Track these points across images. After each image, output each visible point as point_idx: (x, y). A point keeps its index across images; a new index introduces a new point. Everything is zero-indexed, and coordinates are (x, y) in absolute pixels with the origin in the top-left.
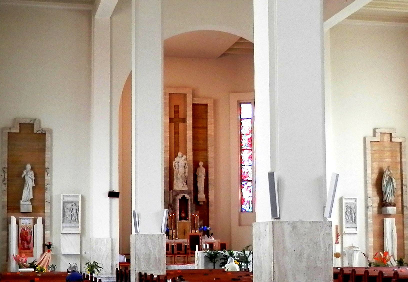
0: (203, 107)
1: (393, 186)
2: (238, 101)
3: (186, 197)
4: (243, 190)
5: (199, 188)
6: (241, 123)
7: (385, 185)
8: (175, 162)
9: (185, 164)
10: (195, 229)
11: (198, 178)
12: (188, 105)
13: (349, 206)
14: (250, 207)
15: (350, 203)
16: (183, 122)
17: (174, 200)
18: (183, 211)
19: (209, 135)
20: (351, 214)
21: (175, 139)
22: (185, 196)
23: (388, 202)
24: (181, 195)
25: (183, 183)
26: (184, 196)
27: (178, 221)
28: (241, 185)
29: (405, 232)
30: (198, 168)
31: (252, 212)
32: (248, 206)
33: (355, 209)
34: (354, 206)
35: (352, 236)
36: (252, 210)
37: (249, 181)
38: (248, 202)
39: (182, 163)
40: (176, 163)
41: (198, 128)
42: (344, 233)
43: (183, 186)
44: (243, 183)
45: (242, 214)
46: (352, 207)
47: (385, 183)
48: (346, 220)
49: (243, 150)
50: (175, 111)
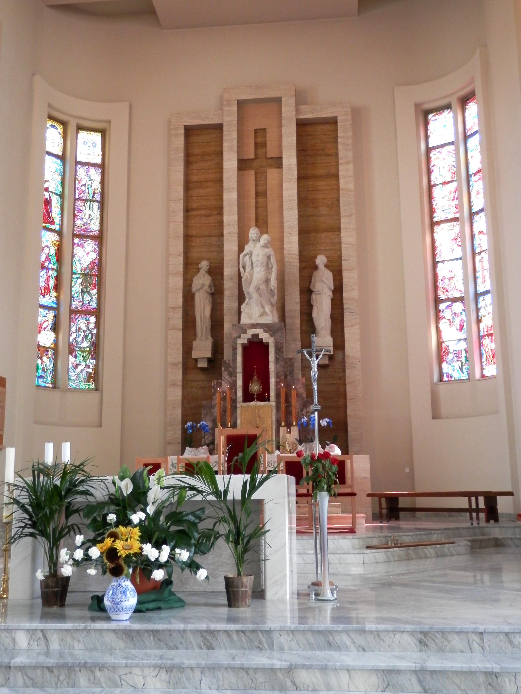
0: (329, 127)
2: (417, 106)
3: (262, 339)
4: (443, 325)
5: (316, 323)
6: (428, 160)
8: (245, 256)
9: (269, 257)
10: (289, 425)
11: (314, 296)
12: (284, 122)
14: (464, 367)
16: (278, 168)
17: (235, 349)
18: (255, 377)
19: (342, 190)
21: (257, 208)
22: (258, 335)
24: (251, 332)
25: (263, 307)
26: (256, 336)
27: (240, 404)
28: (437, 311)
30: (315, 273)
31: (469, 379)
32: (458, 364)
36: (469, 374)
37: (454, 300)
38: (457, 355)
39: (258, 255)
40: (247, 258)
41: (316, 177)
43: (263, 314)
44: (442, 306)
45: (442, 387)
49: (438, 223)
50: (256, 144)
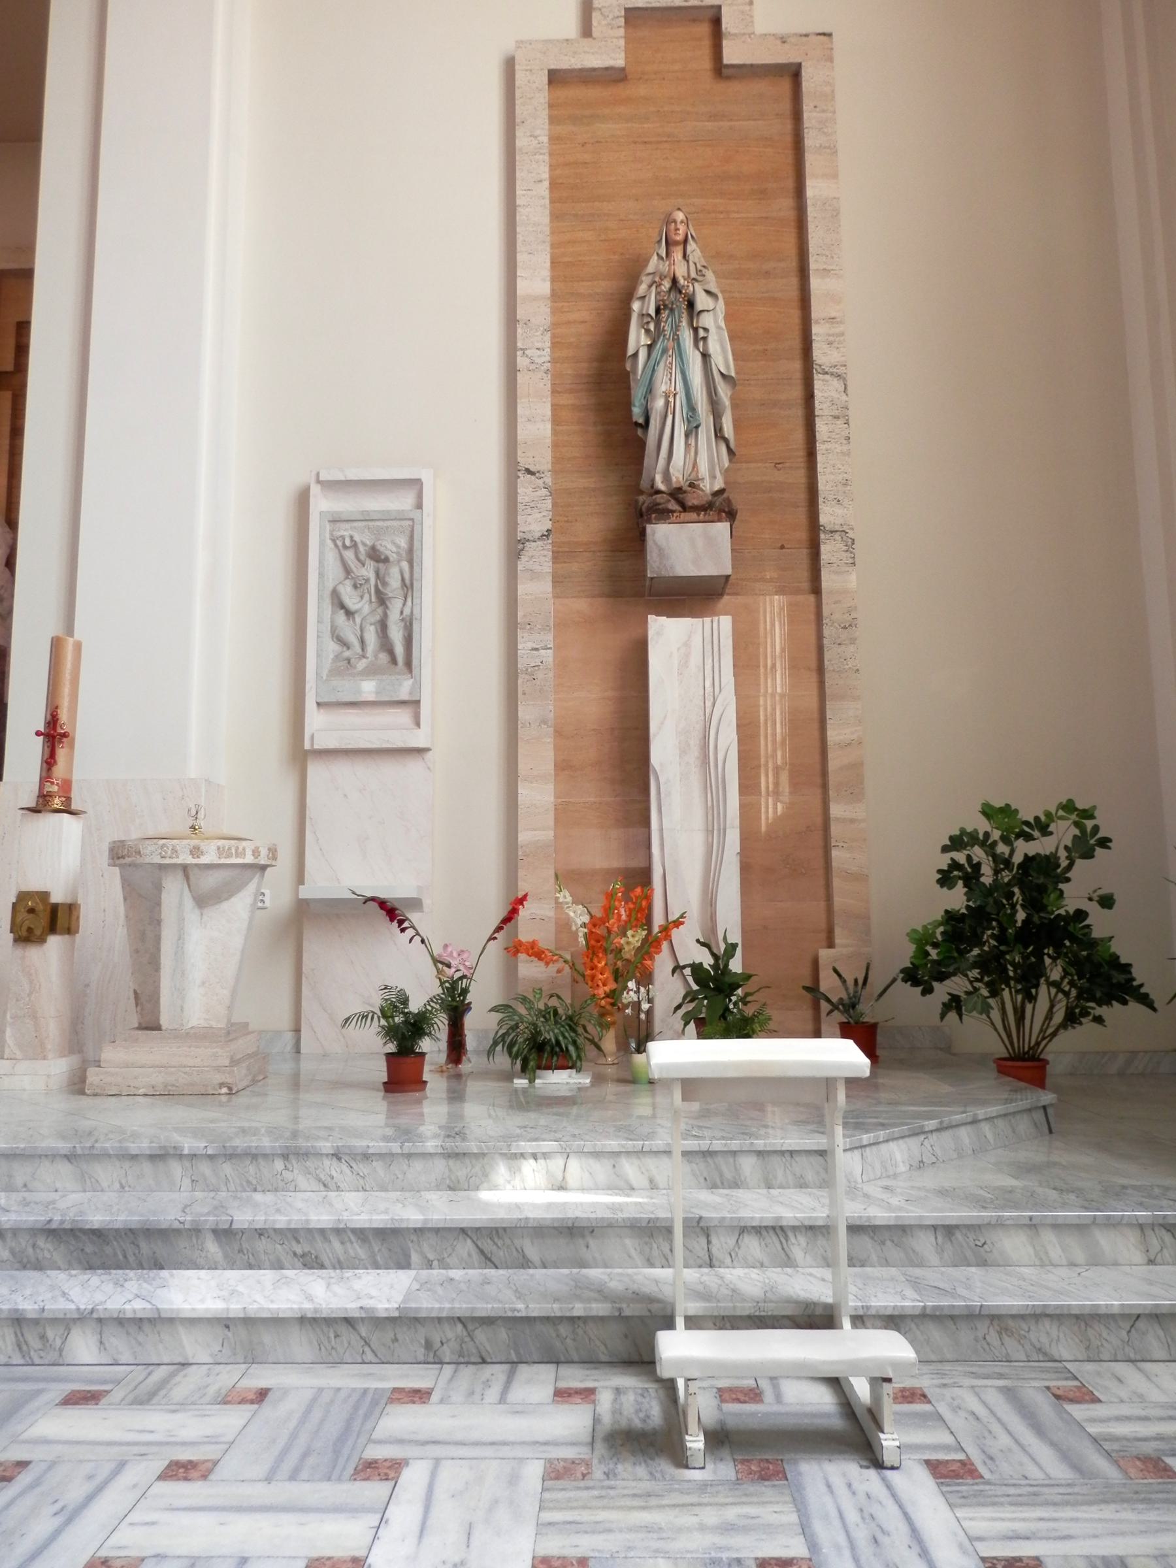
1: (705, 356)
7: (636, 355)
13: (364, 539)
15: (366, 518)
20: (382, 600)
23: (661, 486)
29: (834, 735)
33: (411, 563)
34: (403, 542)
35: (389, 770)
42: (307, 746)
46: (388, 547)
47: (637, 339)
48: (332, 647)
